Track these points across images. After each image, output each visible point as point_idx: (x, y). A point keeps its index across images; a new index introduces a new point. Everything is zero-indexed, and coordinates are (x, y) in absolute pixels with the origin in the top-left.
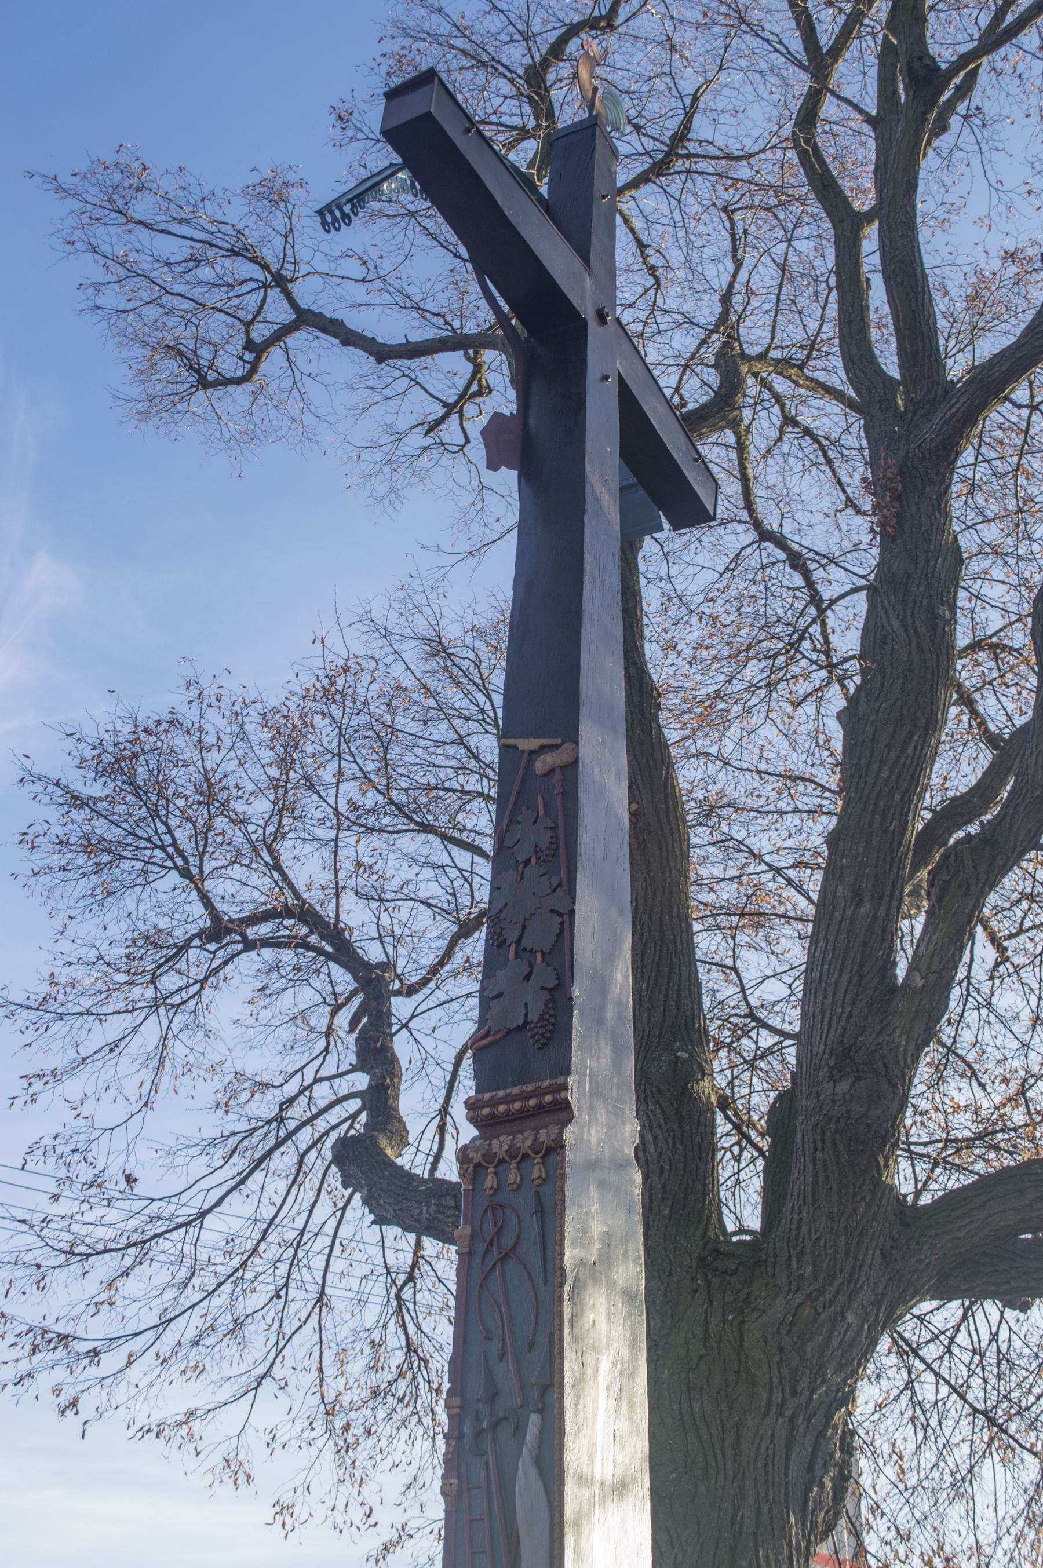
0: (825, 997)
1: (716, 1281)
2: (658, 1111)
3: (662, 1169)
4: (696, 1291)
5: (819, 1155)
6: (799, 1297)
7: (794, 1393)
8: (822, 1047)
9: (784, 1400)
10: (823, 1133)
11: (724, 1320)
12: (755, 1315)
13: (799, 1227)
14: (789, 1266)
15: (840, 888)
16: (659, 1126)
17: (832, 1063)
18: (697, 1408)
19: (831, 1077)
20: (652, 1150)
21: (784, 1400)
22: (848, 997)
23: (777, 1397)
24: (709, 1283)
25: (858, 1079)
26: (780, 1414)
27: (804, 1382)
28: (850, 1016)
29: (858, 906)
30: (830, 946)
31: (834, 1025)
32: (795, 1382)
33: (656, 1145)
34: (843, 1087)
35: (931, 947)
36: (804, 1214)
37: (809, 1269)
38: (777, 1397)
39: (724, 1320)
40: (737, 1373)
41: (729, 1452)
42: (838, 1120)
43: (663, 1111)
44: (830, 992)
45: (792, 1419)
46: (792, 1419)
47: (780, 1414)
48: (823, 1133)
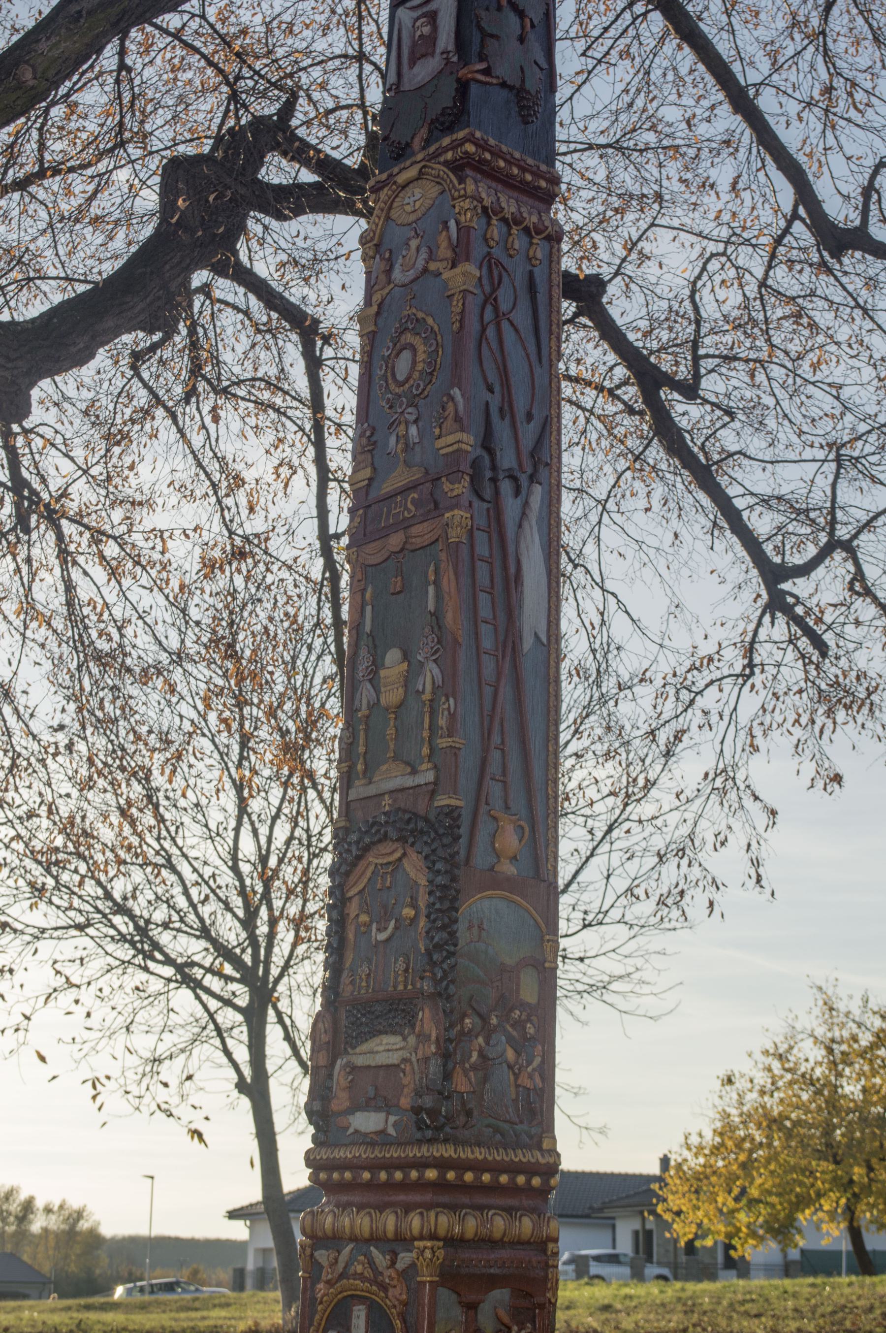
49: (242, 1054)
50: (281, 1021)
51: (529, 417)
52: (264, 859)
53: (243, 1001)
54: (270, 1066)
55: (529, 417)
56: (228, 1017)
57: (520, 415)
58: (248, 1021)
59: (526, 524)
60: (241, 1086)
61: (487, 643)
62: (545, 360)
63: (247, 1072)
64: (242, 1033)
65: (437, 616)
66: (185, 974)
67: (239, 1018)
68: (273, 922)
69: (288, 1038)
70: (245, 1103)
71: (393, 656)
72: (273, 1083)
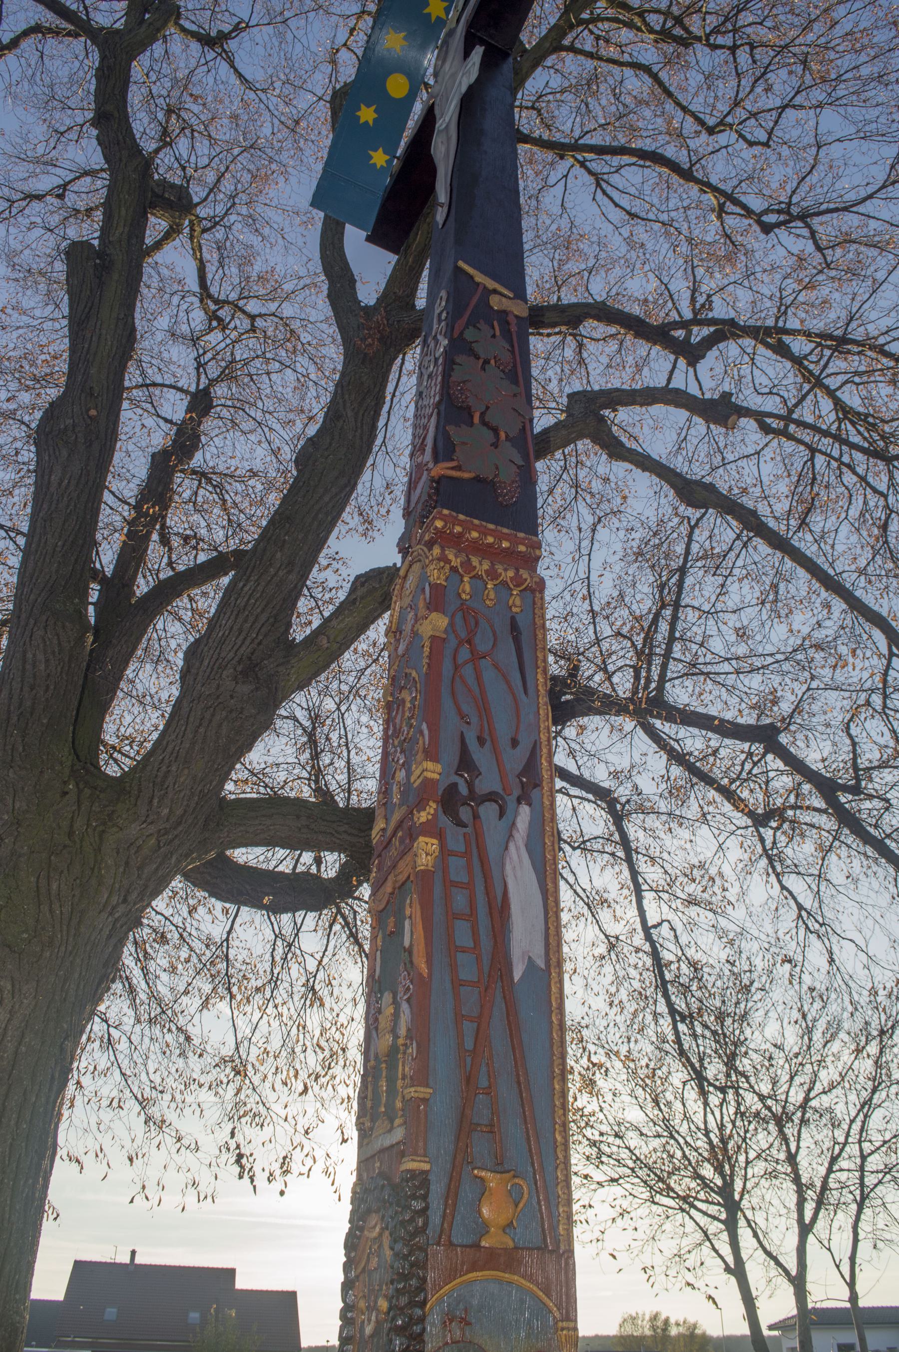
0: (245, 621)
1: (87, 791)
2: (55, 641)
3: (48, 687)
4: (66, 793)
5: (202, 730)
6: (152, 829)
7: (125, 901)
8: (231, 654)
9: (117, 905)
10: (213, 715)
11: (88, 825)
12: (115, 829)
13: (166, 776)
14: (151, 802)
15: (279, 555)
16: (53, 653)
17: (239, 668)
18: (54, 886)
19: (235, 679)
20: (42, 667)
21: (117, 905)
22: (263, 630)
23: (114, 900)
24: (80, 792)
25: (257, 689)
26: (111, 914)
27: (133, 896)
28: (260, 644)
29: (289, 572)
30: (260, 588)
31: (248, 642)
32: (128, 892)
33: (47, 667)
34: (244, 689)
35: (342, 625)
36: (174, 768)
37: (166, 811)
38: (114, 900)
39: (88, 825)
40: (93, 869)
41: (73, 932)
42: (231, 711)
43: (59, 644)
44: (251, 619)
45: (117, 920)
46: (117, 920)
47: (111, 914)
48: (213, 715)
49: (726, 1250)
50: (750, 1226)
51: (515, 743)
52: (721, 1127)
53: (723, 1216)
54: (744, 1256)
55: (515, 743)
56: (714, 1227)
57: (504, 740)
58: (727, 1229)
59: (512, 846)
60: (728, 1269)
61: (468, 972)
62: (531, 690)
63: (730, 1260)
64: (725, 1236)
65: (410, 951)
66: (687, 1201)
67: (722, 1226)
68: (732, 1167)
69: (755, 1235)
70: (733, 1280)
71: (387, 997)
72: (748, 1266)
